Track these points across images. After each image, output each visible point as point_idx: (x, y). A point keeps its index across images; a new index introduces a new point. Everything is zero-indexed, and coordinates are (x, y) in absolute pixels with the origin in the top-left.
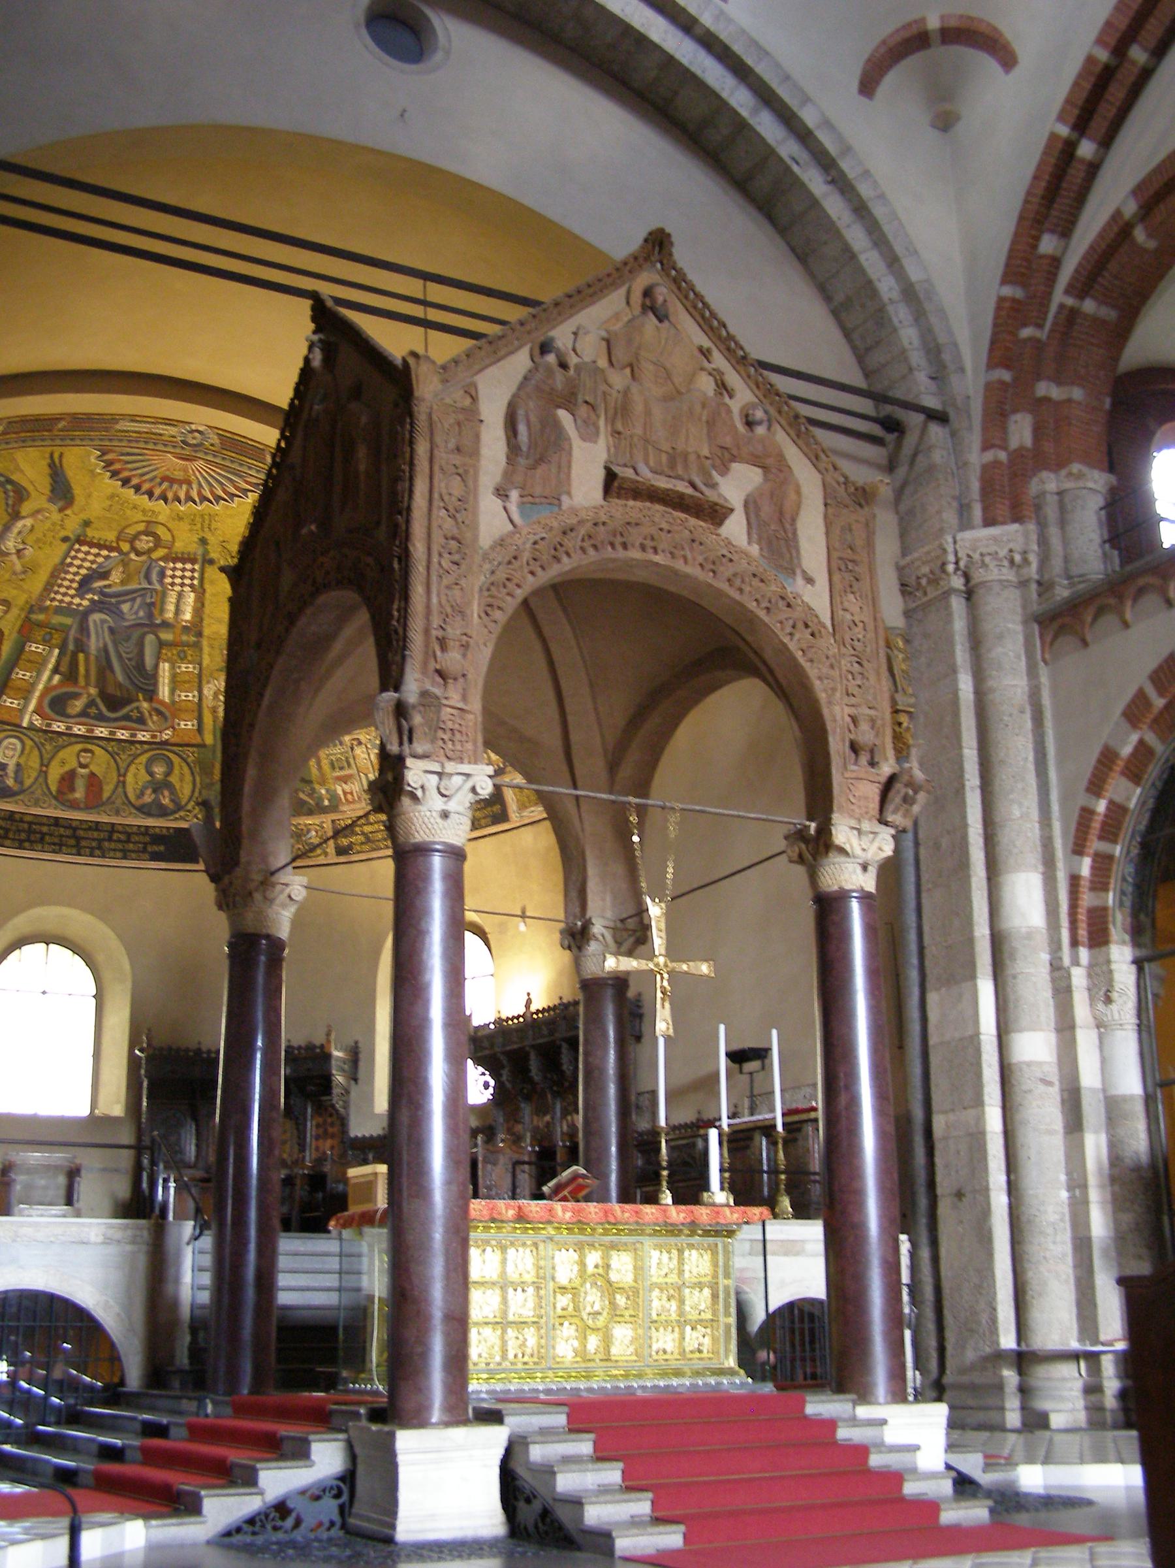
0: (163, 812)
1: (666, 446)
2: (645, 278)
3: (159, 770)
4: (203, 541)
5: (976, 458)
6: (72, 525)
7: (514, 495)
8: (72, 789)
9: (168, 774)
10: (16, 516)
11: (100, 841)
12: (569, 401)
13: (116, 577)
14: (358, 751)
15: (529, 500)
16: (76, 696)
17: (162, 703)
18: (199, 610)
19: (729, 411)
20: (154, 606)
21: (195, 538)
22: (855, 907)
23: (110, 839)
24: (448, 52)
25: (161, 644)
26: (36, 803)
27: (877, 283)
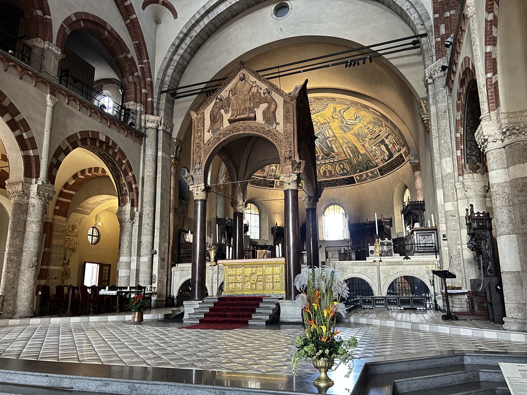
0: (346, 175)
1: (242, 108)
3: (342, 166)
4: (325, 119)
5: (434, 43)
7: (211, 131)
8: (326, 174)
9: (344, 166)
11: (335, 183)
14: (377, 152)
16: (319, 156)
17: (336, 152)
18: (333, 132)
19: (260, 93)
21: (323, 119)
22: (290, 192)
23: (337, 182)
24: (292, 9)
25: (330, 141)
26: (320, 179)
27: (402, 7)
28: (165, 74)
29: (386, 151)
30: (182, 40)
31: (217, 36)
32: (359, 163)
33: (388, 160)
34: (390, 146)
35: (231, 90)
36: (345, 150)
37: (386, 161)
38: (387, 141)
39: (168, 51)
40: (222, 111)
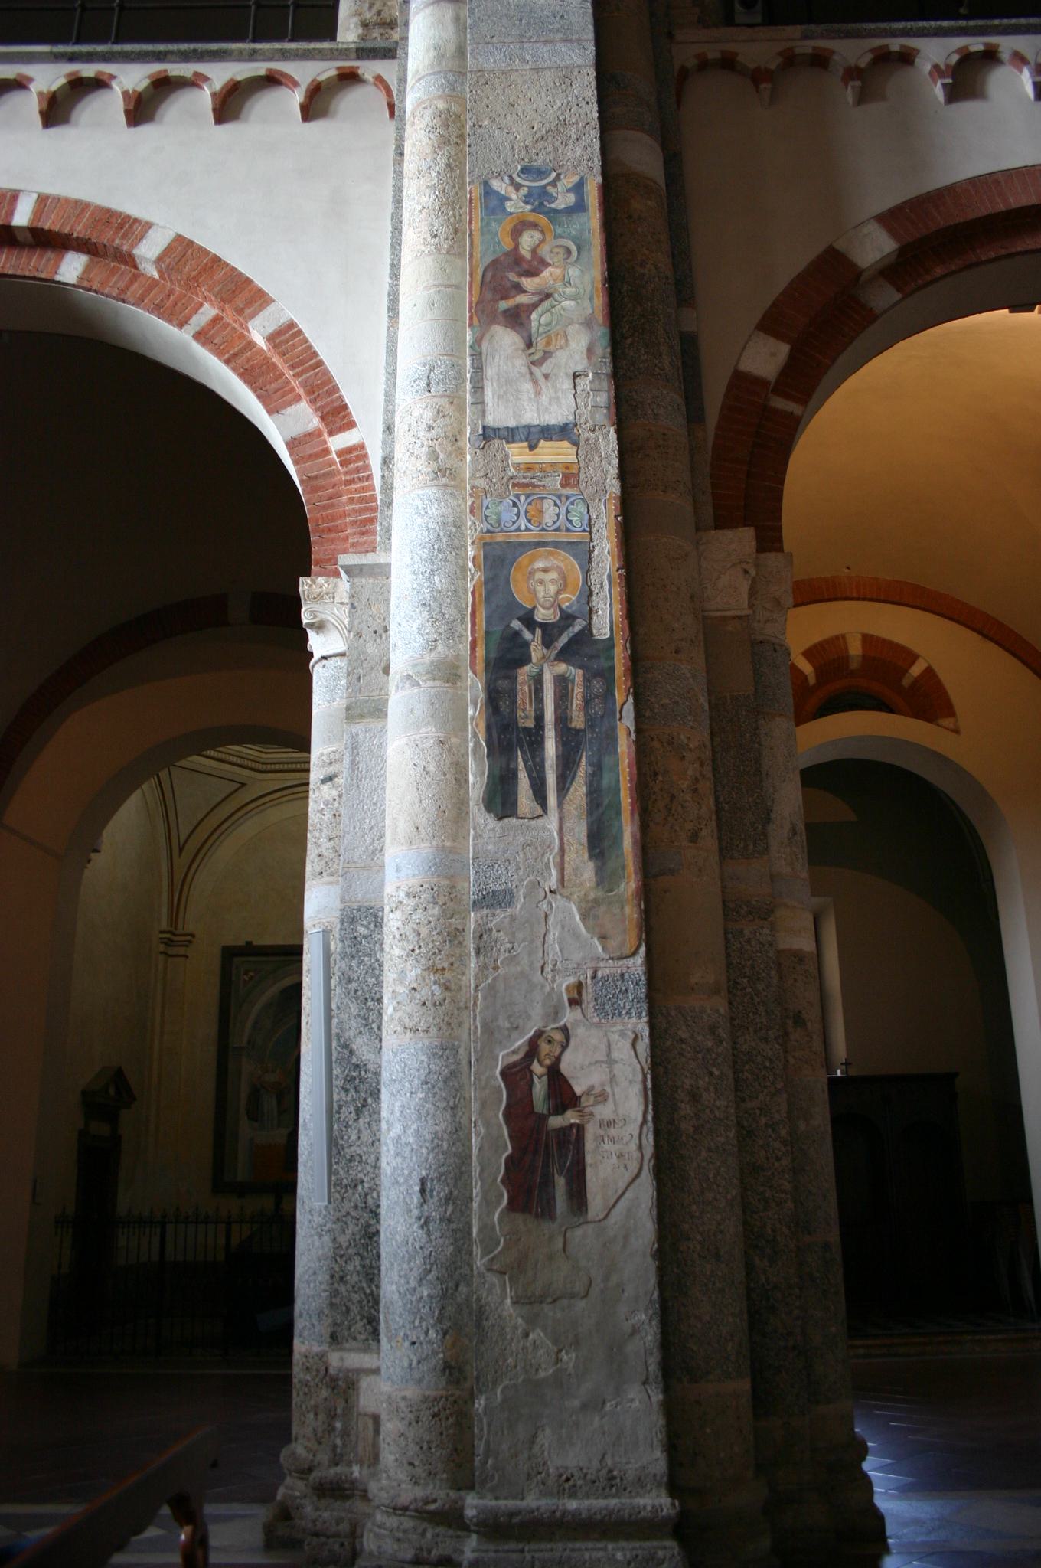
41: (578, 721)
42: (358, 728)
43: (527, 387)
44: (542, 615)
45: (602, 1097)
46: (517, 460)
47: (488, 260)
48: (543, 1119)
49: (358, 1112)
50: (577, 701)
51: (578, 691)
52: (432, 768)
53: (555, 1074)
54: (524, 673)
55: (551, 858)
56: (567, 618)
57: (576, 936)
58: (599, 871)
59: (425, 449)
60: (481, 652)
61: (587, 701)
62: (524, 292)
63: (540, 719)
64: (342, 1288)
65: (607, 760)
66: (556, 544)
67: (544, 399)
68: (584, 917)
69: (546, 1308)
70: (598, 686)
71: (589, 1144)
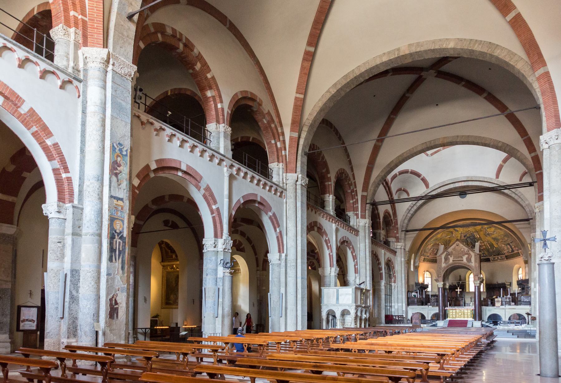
0: (485, 257)
2: (457, 242)
6: (460, 233)
9: (484, 252)
10: (453, 234)
12: (449, 255)
13: (468, 235)
15: (446, 264)
18: (479, 236)
20: (474, 236)
28: (404, 223)
29: (510, 248)
30: (412, 207)
31: (427, 204)
32: (494, 252)
33: (511, 253)
34: (513, 247)
35: (453, 249)
36: (486, 244)
37: (510, 253)
38: (511, 244)
39: (405, 212)
40: (449, 256)
41: (121, 249)
42: (74, 237)
43: (117, 189)
44: (118, 231)
45: (121, 303)
46: (115, 202)
47: (113, 161)
48: (114, 306)
49: (73, 303)
50: (121, 246)
51: (121, 244)
52: (97, 251)
53: (115, 300)
54: (115, 240)
55: (117, 269)
56: (121, 232)
57: (119, 281)
58: (123, 272)
59: (97, 193)
60: (109, 235)
61: (122, 246)
62: (118, 170)
63: (116, 248)
64: (70, 330)
65: (124, 256)
66: (120, 219)
67: (120, 192)
68: (120, 278)
69: (113, 331)
70: (124, 244)
71: (119, 310)
